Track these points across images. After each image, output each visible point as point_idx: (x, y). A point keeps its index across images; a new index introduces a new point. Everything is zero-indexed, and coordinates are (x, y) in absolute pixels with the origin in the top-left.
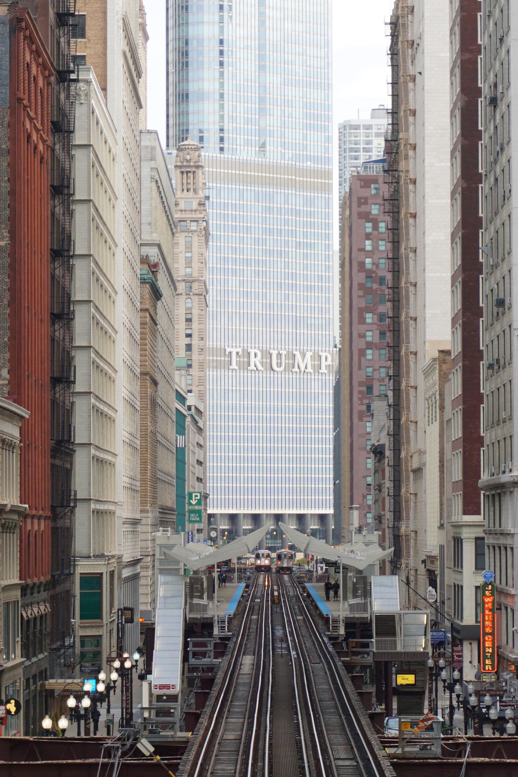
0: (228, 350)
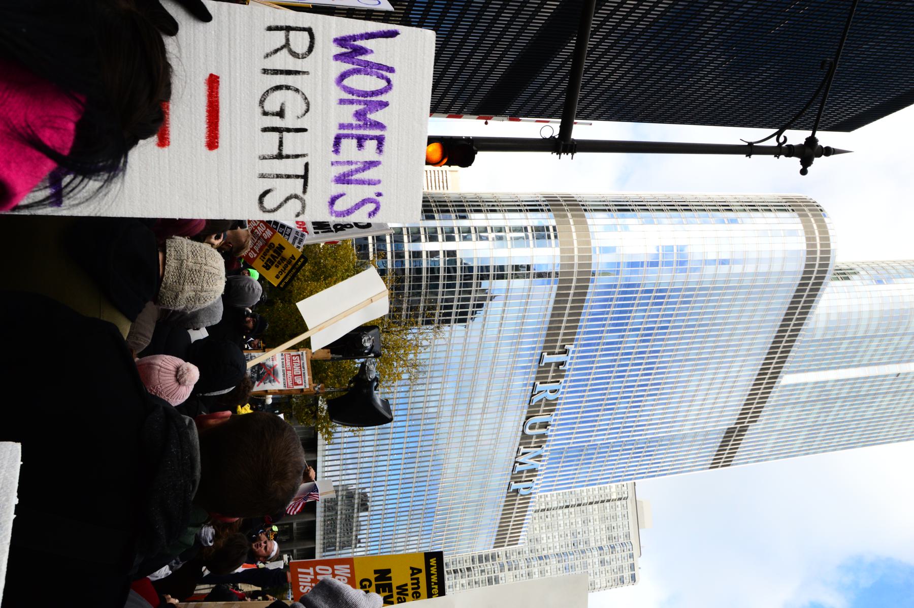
0: (570, 347)
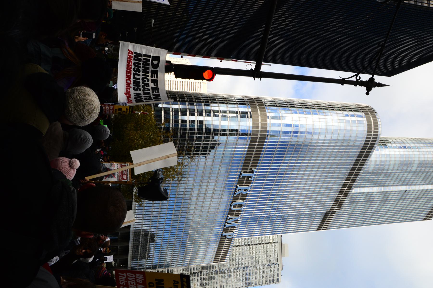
0: (255, 170)
